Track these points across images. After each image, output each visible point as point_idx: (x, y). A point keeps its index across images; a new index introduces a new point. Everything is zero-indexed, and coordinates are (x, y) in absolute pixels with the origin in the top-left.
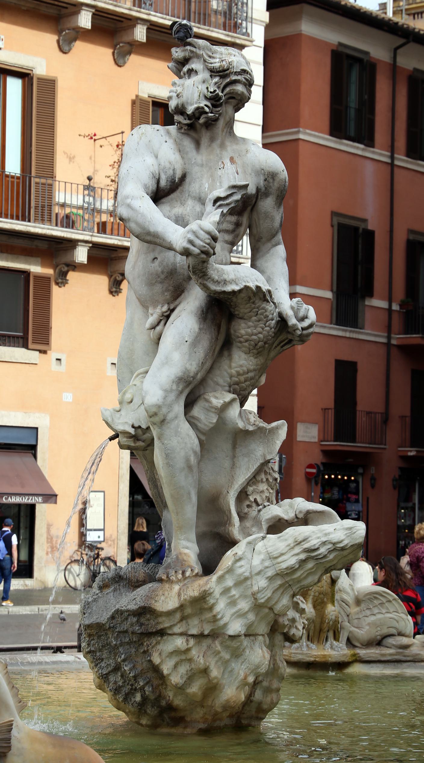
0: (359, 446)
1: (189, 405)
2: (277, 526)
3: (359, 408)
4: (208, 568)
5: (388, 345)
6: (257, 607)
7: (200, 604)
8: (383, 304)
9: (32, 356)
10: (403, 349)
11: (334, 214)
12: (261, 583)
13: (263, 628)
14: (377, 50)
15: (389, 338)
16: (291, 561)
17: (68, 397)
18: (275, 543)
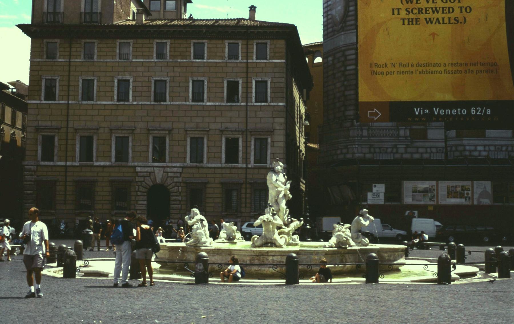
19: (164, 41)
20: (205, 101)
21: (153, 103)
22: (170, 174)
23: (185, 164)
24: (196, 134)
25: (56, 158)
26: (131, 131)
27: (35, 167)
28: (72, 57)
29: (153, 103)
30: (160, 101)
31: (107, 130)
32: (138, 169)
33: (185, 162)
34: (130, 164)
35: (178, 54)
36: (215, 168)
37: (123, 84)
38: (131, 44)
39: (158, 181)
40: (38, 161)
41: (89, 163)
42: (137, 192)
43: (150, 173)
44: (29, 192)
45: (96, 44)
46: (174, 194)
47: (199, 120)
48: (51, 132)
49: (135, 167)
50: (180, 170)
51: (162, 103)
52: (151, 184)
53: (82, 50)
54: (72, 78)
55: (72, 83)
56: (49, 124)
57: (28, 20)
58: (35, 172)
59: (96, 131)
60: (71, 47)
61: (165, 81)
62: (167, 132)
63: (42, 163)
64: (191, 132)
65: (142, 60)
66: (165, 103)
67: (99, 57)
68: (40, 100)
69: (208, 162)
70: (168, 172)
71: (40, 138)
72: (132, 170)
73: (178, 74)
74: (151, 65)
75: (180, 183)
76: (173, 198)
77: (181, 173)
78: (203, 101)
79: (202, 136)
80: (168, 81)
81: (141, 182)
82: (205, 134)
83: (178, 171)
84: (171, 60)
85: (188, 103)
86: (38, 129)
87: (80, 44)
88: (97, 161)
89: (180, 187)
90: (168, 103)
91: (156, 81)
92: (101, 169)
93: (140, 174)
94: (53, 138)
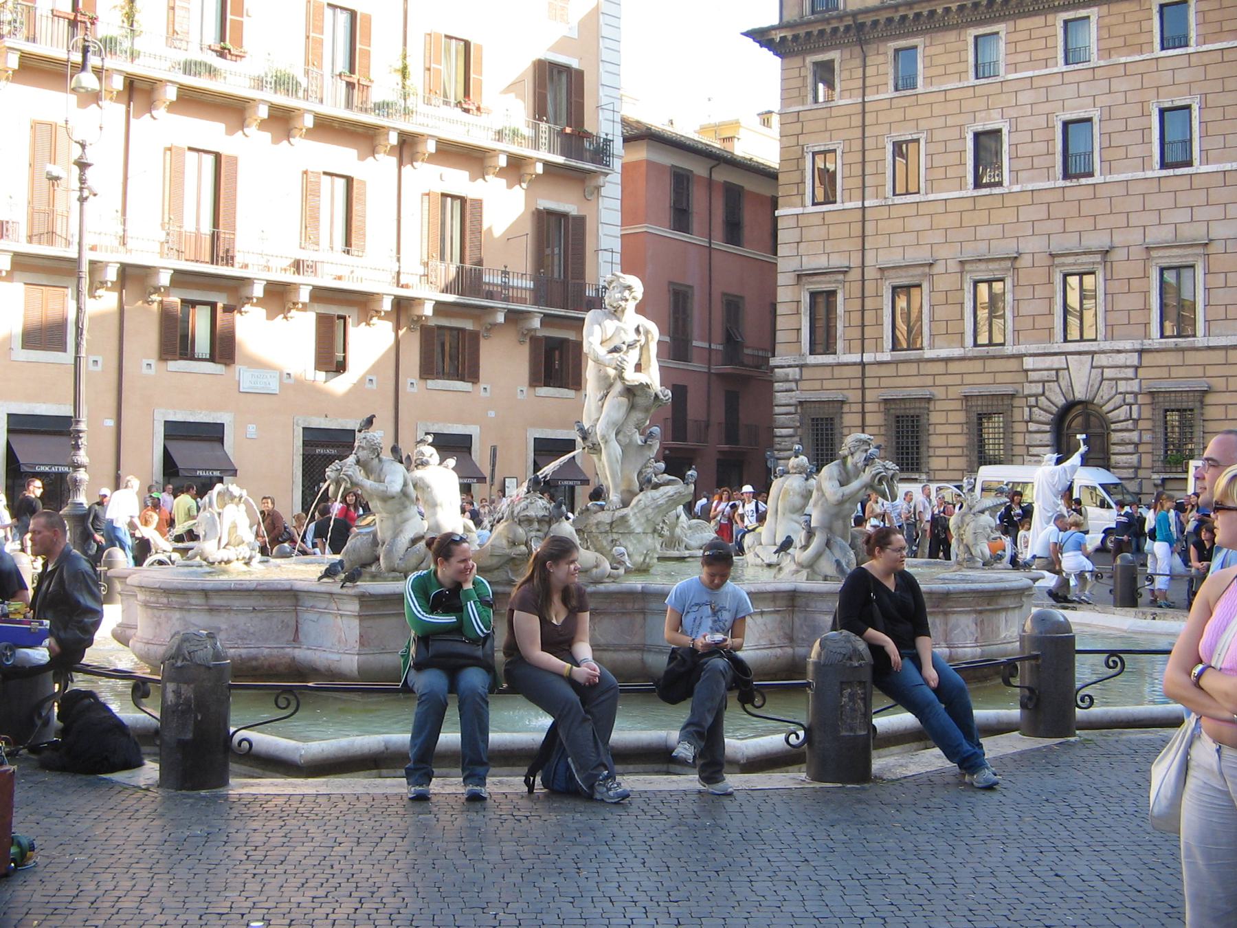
0: (690, 444)
1: (617, 434)
2: (656, 486)
3: (689, 417)
4: (625, 504)
5: (709, 373)
6: (648, 520)
7: (623, 519)
8: (706, 345)
9: (467, 386)
10: (721, 376)
11: (670, 283)
12: (650, 510)
13: (650, 530)
14: (698, 168)
15: (709, 368)
16: (661, 501)
17: (492, 414)
18: (655, 493)
19: (1082, 13)
20: (1196, 162)
21: (1061, 183)
22: (1108, 373)
23: (1146, 342)
24: (1174, 257)
25: (840, 345)
26: (1009, 264)
27: (797, 369)
28: (867, 90)
29: (1061, 183)
30: (1078, 176)
31: (953, 266)
32: (1029, 363)
33: (1147, 336)
34: (1009, 349)
35: (1120, 42)
36: (1226, 348)
37: (986, 143)
38: (1002, 34)
39: (1080, 394)
40: (802, 355)
41: (913, 354)
42: (1027, 422)
43: (1057, 370)
44: (784, 431)
45: (920, 50)
46: (1119, 426)
47: (1182, 216)
48: (829, 282)
49: (1020, 356)
50: (1133, 359)
51: (1083, 181)
52: (1061, 401)
53: (891, 71)
54: (869, 143)
55: (869, 156)
56: (821, 262)
57: (769, 17)
58: (796, 381)
59: (927, 269)
60: (864, 67)
61: (1089, 120)
62: (1098, 258)
63: (812, 360)
64: (1161, 253)
65: (1030, 74)
66: (1090, 181)
67: (930, 79)
68: (803, 206)
69: (1208, 334)
70: (1103, 367)
71: (805, 299)
72: (1013, 365)
73: (1120, 98)
74: (1053, 83)
75: (1136, 394)
76: (1115, 437)
77: (1136, 368)
78: (1189, 164)
79: (1190, 261)
80: (1096, 120)
81: (1036, 396)
82: (1198, 255)
83: (1128, 363)
84: (1102, 63)
85: (1149, 174)
86: (800, 277)
87: (886, 53)
88: (932, 347)
89: (1135, 408)
90: (1097, 178)
91: (1066, 124)
92: (940, 367)
93: (1033, 376)
94: (833, 293)
